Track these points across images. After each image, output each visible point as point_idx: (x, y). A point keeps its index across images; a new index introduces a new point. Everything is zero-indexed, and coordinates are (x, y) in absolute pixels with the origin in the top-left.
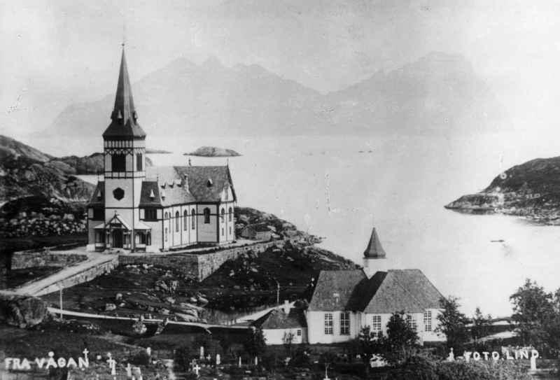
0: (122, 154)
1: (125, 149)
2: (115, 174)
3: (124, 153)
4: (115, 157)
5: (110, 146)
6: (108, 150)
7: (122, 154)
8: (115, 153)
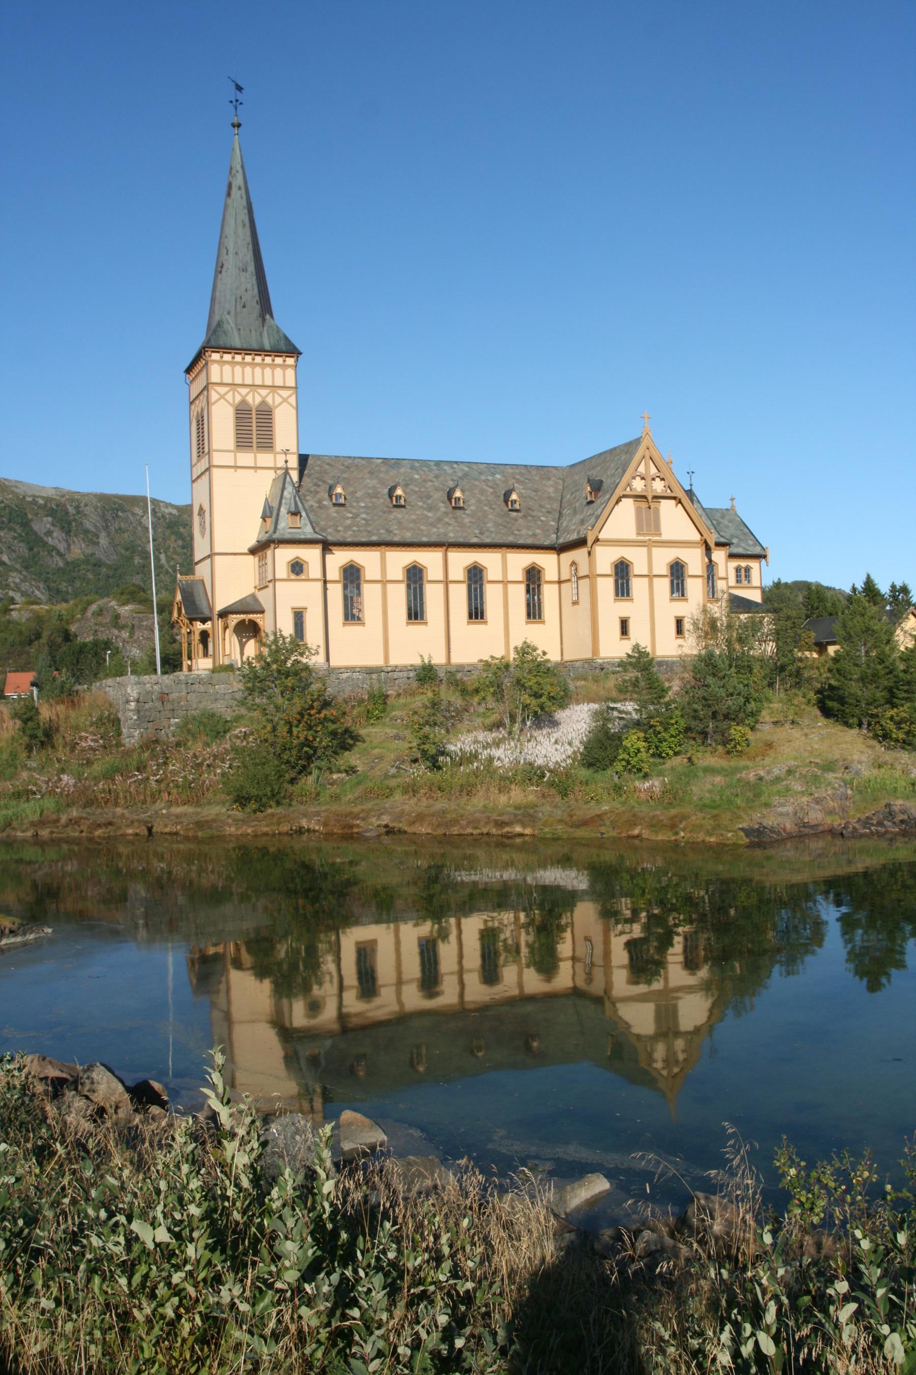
0: (263, 402)
1: (273, 387)
2: (245, 458)
3: (269, 400)
4: (242, 413)
5: (227, 379)
6: (223, 390)
7: (263, 402)
8: (244, 402)
